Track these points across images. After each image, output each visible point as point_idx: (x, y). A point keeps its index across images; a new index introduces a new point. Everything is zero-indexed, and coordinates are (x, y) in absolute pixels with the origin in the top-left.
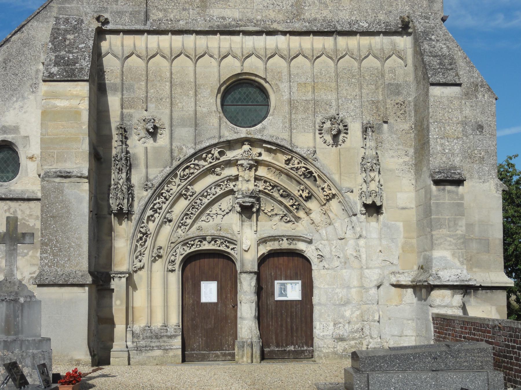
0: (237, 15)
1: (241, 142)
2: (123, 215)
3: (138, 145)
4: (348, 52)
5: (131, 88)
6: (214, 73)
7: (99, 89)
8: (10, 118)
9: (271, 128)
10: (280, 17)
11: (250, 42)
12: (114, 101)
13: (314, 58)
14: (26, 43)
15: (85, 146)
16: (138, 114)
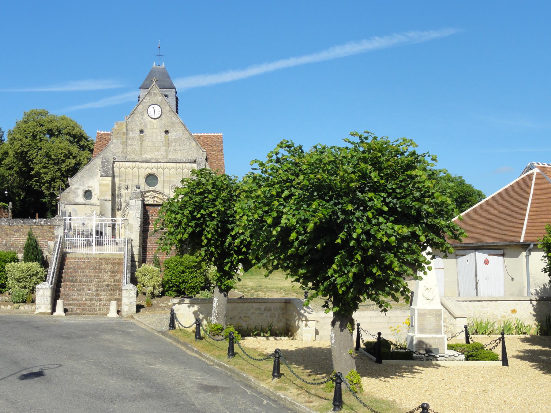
0: (150, 157)
1: (150, 191)
2: (119, 209)
3: (123, 191)
4: (180, 168)
5: (121, 176)
6: (144, 173)
7: (113, 176)
8: (90, 184)
9: (158, 187)
10: (162, 158)
11: (153, 164)
12: (117, 180)
13: (170, 169)
14: (94, 164)
15: (111, 193)
16: (123, 183)
